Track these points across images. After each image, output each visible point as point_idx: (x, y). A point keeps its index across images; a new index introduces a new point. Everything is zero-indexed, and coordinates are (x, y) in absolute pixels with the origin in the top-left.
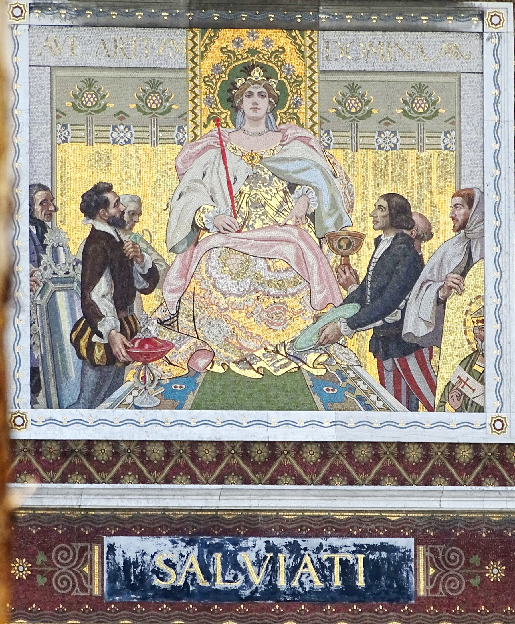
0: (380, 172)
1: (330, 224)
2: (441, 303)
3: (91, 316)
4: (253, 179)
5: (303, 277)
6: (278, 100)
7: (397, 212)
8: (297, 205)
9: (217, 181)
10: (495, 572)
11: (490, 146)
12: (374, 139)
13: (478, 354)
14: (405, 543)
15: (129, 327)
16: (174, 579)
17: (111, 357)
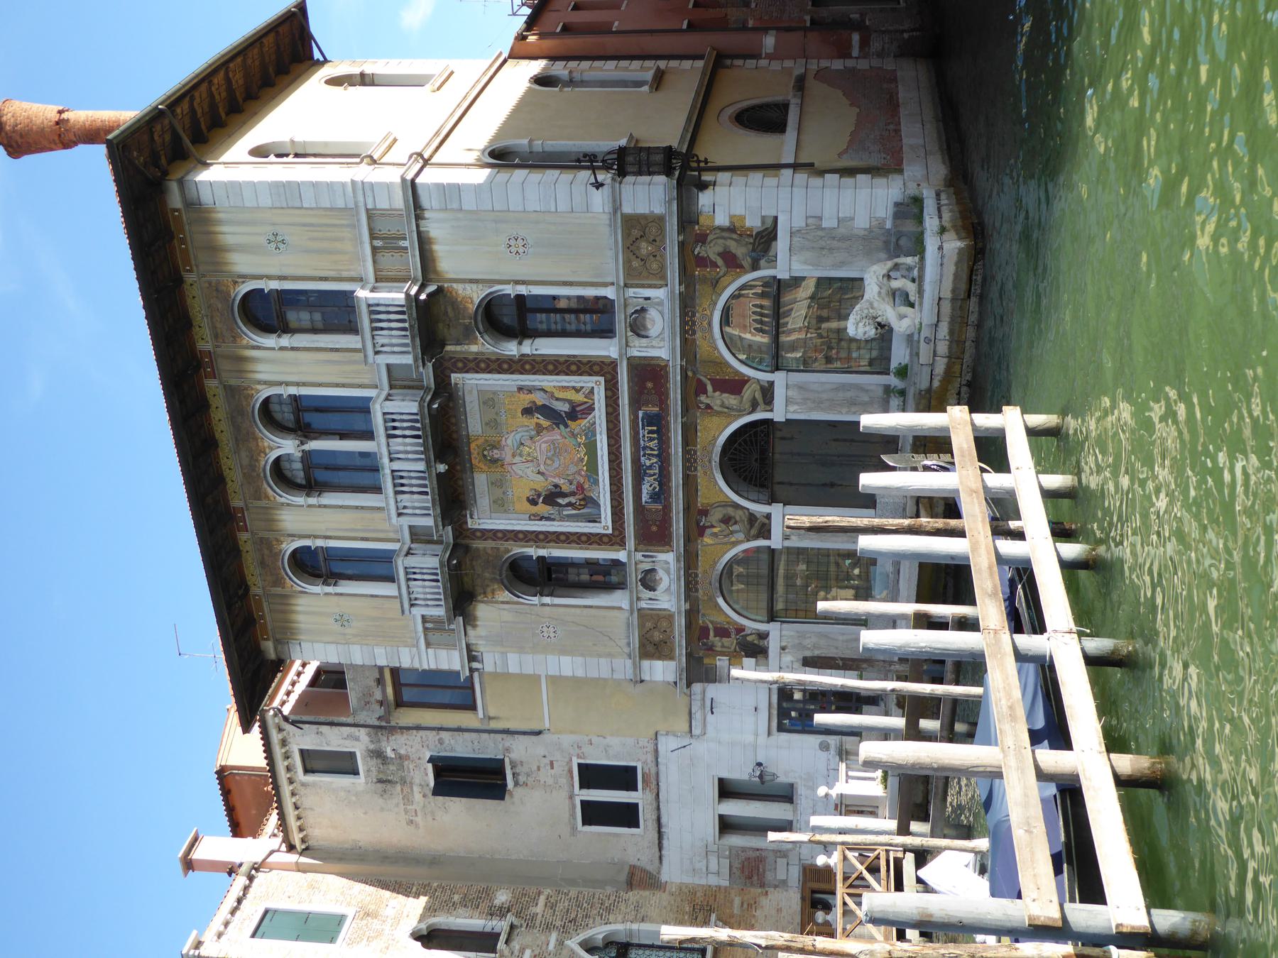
0: (514, 417)
1: (533, 433)
2: (557, 399)
3: (569, 504)
4: (521, 455)
5: (553, 442)
6: (494, 447)
7: (527, 411)
8: (528, 443)
9: (523, 466)
10: (650, 385)
11: (501, 382)
13: (574, 388)
14: (641, 414)
15: (573, 494)
17: (583, 499)
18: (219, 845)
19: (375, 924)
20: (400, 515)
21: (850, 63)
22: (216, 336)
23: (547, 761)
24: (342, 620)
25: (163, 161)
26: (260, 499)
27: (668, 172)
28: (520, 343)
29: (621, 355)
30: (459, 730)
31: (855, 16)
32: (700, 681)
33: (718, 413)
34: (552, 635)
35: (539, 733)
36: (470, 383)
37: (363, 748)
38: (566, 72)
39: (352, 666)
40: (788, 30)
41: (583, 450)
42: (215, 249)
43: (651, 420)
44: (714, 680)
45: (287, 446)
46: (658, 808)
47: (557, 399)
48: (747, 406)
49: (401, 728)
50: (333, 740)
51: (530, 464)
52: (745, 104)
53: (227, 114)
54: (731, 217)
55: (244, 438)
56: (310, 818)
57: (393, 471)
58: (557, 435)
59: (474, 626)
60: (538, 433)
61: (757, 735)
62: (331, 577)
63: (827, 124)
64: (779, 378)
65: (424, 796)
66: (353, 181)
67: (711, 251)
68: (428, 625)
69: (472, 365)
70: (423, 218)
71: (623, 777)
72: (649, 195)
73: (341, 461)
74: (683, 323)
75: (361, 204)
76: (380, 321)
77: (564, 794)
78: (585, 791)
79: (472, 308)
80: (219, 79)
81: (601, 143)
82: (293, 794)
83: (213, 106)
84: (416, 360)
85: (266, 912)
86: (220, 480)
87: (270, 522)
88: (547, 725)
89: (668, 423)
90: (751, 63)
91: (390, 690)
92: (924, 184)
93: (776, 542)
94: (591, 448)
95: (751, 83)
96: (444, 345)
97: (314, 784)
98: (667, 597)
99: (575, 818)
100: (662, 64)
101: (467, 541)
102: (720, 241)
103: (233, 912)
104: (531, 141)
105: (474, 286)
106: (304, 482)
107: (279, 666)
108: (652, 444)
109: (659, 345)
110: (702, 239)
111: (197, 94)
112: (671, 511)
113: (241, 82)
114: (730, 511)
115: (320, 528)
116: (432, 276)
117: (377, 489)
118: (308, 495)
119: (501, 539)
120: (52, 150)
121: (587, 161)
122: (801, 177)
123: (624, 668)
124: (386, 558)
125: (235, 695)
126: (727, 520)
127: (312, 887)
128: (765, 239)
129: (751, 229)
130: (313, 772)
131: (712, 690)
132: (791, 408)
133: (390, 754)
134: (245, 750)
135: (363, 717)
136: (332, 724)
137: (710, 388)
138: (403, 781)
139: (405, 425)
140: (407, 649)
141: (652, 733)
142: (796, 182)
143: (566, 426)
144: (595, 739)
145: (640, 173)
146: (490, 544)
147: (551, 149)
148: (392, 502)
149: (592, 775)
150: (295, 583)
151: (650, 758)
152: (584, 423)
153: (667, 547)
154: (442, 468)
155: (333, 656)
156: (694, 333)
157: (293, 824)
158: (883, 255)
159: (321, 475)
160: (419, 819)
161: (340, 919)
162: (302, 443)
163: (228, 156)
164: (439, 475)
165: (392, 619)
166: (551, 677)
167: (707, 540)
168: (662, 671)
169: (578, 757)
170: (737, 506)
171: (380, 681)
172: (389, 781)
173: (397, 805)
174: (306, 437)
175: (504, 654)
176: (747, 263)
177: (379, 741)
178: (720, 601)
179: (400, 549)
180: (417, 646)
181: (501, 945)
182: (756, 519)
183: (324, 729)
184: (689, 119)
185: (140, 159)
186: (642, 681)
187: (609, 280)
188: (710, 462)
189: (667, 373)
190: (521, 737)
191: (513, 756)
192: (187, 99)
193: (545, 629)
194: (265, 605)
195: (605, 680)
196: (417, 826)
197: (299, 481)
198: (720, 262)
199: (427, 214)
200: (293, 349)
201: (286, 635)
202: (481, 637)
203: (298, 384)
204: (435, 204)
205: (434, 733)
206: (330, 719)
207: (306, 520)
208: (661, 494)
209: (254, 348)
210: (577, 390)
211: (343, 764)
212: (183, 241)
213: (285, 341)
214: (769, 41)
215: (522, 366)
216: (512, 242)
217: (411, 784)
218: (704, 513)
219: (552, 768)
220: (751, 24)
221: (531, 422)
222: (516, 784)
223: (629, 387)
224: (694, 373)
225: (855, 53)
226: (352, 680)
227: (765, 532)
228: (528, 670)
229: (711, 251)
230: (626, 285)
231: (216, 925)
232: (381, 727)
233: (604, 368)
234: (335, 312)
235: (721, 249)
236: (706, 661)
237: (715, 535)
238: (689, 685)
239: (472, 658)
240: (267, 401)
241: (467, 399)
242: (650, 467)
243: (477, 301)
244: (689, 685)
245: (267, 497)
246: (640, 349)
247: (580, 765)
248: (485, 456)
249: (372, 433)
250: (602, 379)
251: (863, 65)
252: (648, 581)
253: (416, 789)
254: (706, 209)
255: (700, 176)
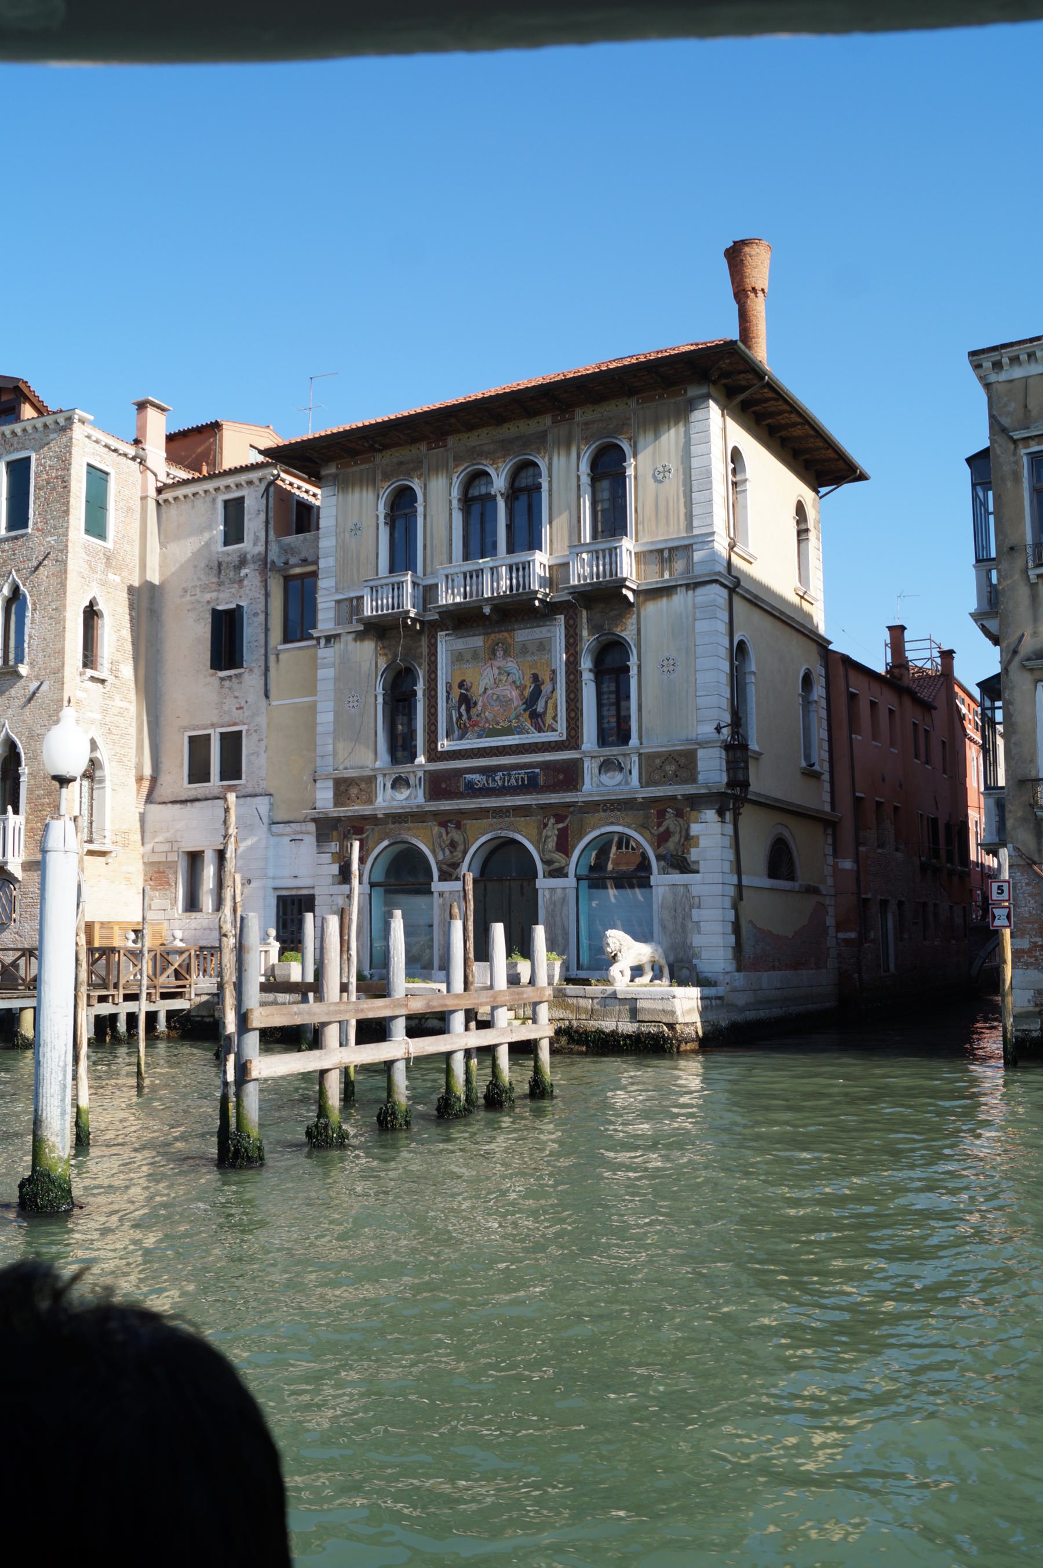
0: (531, 667)
2: (546, 702)
3: (460, 715)
4: (499, 674)
7: (535, 678)
8: (510, 679)
9: (491, 675)
10: (561, 777)
12: (529, 659)
13: (556, 715)
15: (469, 718)
16: (480, 785)
18: (157, 428)
19: (100, 566)
20: (447, 577)
21: (832, 931)
22: (586, 424)
23: (243, 704)
24: (356, 529)
25: (724, 381)
26: (455, 460)
27: (730, 784)
28: (590, 670)
29: (584, 752)
30: (267, 630)
31: (872, 935)
32: (317, 829)
33: (540, 834)
34: (351, 705)
35: (267, 696)
36: (557, 631)
37: (248, 549)
38: (816, 698)
39: (317, 539)
40: (858, 880)
41: (506, 724)
42: (656, 424)
43: (533, 778)
44: (318, 841)
45: (499, 482)
46: (207, 799)
47: (546, 702)
48: (547, 857)
49: (266, 581)
50: (253, 524)
51: (492, 682)
52: (793, 846)
53: (768, 425)
54: (698, 837)
55: (505, 448)
56: (185, 507)
57: (482, 570)
58: (517, 702)
59: (355, 640)
60: (517, 688)
61: (274, 878)
62: (392, 520)
63: (778, 913)
64: (570, 882)
65: (208, 602)
66: (713, 533)
67: (670, 822)
68: (355, 602)
69: (571, 632)
70: (687, 591)
71: (232, 769)
72: (712, 769)
73: (488, 526)
74: (612, 802)
75: (696, 540)
76: (604, 558)
77: (215, 720)
78: (218, 737)
79: (617, 630)
80: (794, 418)
81: (755, 730)
82: (206, 492)
83: (772, 415)
84: (574, 587)
85: (107, 474)
86: (471, 428)
87: (437, 468)
88: (274, 703)
89: (531, 793)
90: (829, 850)
91: (298, 570)
92: (728, 988)
93: (437, 886)
94: (508, 731)
95: (808, 846)
96: (587, 608)
97: (214, 509)
98: (387, 799)
99: (194, 730)
100: (826, 777)
101: (426, 633)
102: (678, 829)
103: (106, 446)
104: (754, 673)
105: (635, 632)
106: (470, 495)
107: (315, 477)
108: (513, 781)
109: (595, 784)
110: (679, 814)
111: (780, 403)
112: (459, 798)
113: (795, 434)
114: (461, 847)
115: (433, 510)
116: (641, 598)
117: (466, 557)
118: (459, 500)
119: (430, 659)
120: (733, 283)
121: (737, 721)
122: (731, 891)
123: (327, 766)
124: (410, 565)
125: (291, 444)
126: (453, 845)
127: (129, 509)
128: (682, 865)
129: (689, 853)
130: (225, 508)
131: (310, 840)
132: (547, 893)
133: (244, 572)
134: (238, 448)
135: (274, 548)
136: (267, 522)
137: (561, 826)
138: (220, 584)
139: (521, 580)
140: (333, 584)
141: (271, 791)
142: (727, 887)
143: (525, 710)
144: (264, 743)
145: (728, 763)
146: (425, 651)
147: (748, 690)
148: (457, 570)
149: (232, 743)
150: (386, 492)
151: (250, 790)
152: (528, 725)
153: (428, 797)
154: (487, 610)
155: (326, 521)
156: (604, 811)
157: (180, 492)
158: (671, 959)
159: (476, 509)
160: (188, 598)
161: (102, 535)
162: (502, 495)
163: (732, 425)
164: (481, 608)
165: (358, 571)
166: (315, 705)
167: (436, 829)
168: (324, 797)
169: (248, 731)
170: (465, 852)
171: (305, 562)
172: (220, 572)
173: (199, 579)
174: (508, 497)
175: (333, 665)
176: (662, 851)
177: (254, 562)
178: (386, 843)
179: (418, 577)
180: (337, 591)
181: (90, 672)
182: (455, 869)
183: (263, 516)
184: (777, 800)
185: (725, 364)
186: (315, 781)
187: (644, 741)
188: (501, 829)
189: (571, 791)
190: (262, 682)
191: (246, 676)
192: (775, 396)
193: (355, 698)
194: (366, 466)
195: (315, 750)
196: (183, 596)
197: (471, 491)
198: (662, 829)
199: (690, 592)
200: (579, 486)
201: (342, 484)
202: (346, 645)
203: (550, 490)
204: (699, 599)
205: (263, 609)
206: (272, 522)
207: (438, 499)
208: (472, 791)
209: (578, 455)
210: (555, 718)
211: (234, 533)
212: (661, 397)
213: (585, 480)
214: (847, 864)
215: (572, 673)
216: (671, 662)
217: (219, 591)
218: (458, 826)
219: (237, 709)
220: (862, 849)
221: (528, 682)
222: (222, 679)
223: (558, 760)
224: (571, 813)
225: (841, 935)
226: (305, 539)
227: (445, 877)
228: (320, 686)
229: (670, 822)
230: (640, 754)
231: (97, 434)
232: (266, 564)
233: (573, 740)
234: (612, 521)
235: (672, 829)
236: (335, 833)
237: (440, 836)
238: (314, 820)
239: (328, 639)
240: (536, 465)
241: (544, 629)
242: (494, 780)
243: (623, 634)
244: (314, 820)
245: (456, 466)
246: (590, 768)
247: (240, 732)
248: (497, 644)
249: (513, 552)
250: (564, 738)
251: (831, 942)
252: (399, 782)
253: (214, 595)
254: (703, 816)
255: (729, 810)
